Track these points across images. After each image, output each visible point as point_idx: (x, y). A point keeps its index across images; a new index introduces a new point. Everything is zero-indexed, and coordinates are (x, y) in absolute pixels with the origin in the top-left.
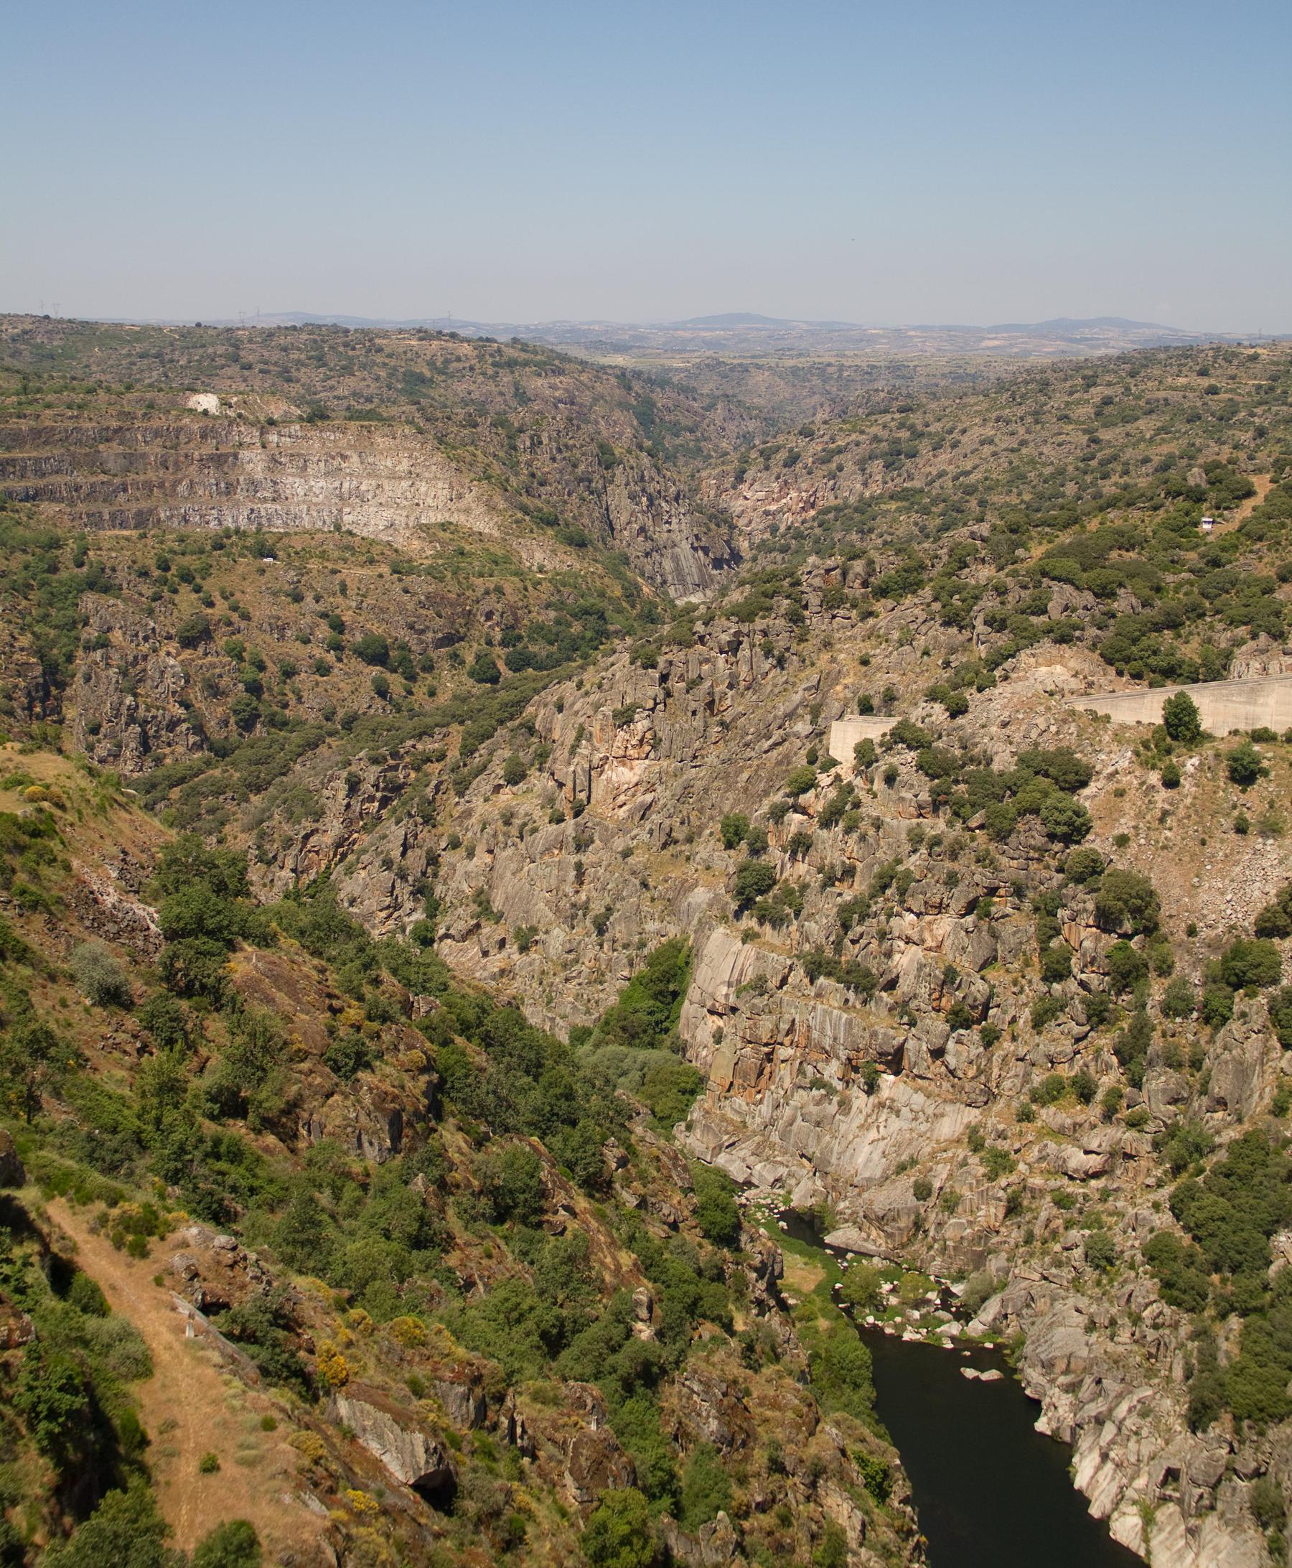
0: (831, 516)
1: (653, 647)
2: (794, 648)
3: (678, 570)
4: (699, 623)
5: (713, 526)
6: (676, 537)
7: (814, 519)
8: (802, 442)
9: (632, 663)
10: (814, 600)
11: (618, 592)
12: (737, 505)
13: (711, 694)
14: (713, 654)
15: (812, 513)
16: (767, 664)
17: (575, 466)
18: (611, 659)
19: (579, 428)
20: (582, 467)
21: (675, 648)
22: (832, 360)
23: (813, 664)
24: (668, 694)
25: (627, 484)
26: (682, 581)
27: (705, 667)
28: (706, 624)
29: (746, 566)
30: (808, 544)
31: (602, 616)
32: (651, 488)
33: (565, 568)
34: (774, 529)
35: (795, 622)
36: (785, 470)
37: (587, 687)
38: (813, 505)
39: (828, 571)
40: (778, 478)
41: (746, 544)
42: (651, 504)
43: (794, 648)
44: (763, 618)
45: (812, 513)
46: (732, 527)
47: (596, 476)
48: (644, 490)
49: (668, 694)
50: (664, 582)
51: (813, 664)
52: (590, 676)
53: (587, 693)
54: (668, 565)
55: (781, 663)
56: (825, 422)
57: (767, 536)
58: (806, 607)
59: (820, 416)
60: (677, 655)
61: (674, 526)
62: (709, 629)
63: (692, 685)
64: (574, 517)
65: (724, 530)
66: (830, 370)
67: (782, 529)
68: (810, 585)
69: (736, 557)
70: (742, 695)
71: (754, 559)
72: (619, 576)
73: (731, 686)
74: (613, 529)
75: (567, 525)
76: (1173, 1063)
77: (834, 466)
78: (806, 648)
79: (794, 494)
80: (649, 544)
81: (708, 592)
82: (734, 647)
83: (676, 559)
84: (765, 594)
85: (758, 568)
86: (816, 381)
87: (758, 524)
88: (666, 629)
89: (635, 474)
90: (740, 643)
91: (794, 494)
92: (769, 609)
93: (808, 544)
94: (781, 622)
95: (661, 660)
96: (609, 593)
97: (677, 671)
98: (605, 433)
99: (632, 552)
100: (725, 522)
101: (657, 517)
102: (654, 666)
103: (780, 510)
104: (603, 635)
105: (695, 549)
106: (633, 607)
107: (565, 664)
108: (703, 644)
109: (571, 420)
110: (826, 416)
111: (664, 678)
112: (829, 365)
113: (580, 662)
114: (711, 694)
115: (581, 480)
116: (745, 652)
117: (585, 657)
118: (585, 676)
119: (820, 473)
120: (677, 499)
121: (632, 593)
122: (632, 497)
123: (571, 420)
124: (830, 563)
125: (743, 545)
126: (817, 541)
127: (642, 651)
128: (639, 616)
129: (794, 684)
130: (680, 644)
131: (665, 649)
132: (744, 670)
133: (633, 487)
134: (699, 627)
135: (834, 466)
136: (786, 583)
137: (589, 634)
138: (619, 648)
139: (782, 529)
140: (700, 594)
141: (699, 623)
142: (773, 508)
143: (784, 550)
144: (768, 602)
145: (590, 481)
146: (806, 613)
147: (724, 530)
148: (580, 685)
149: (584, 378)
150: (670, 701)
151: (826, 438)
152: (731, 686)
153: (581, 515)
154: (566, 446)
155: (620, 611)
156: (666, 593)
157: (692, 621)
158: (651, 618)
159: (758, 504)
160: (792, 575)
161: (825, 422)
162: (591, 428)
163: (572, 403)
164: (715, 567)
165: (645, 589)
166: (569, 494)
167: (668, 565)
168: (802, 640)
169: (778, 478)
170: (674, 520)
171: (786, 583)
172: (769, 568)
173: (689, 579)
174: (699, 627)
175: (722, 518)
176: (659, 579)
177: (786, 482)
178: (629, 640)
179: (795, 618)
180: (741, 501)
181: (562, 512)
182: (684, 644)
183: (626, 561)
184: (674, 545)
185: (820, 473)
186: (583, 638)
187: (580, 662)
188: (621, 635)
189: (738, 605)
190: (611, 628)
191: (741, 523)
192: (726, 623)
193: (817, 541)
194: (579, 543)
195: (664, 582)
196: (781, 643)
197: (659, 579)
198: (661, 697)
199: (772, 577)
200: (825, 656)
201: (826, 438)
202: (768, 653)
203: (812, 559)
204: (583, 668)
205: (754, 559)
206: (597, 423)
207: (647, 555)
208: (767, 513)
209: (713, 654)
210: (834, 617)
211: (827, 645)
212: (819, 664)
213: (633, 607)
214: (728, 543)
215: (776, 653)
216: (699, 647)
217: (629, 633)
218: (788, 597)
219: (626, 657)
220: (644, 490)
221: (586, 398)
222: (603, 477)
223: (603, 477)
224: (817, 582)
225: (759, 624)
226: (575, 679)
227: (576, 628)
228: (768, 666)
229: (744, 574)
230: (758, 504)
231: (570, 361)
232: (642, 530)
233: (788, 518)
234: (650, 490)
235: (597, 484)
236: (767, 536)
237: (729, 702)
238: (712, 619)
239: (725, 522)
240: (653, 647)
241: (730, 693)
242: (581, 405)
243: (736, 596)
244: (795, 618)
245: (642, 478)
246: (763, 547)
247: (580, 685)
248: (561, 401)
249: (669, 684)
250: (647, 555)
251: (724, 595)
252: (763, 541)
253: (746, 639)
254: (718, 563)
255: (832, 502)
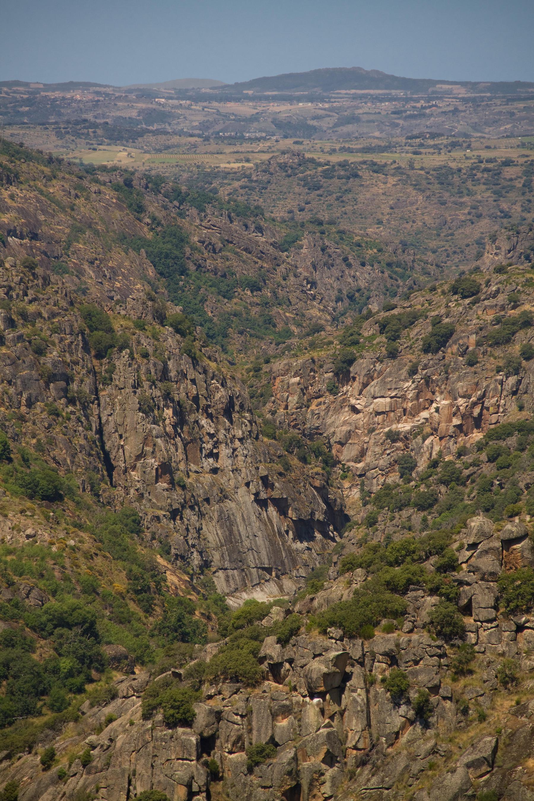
0: (512, 441)
1: (186, 685)
2: (448, 685)
3: (231, 540)
4: (270, 640)
5: (295, 461)
6: (227, 480)
7: (480, 446)
8: (458, 306)
9: (146, 717)
10: (482, 596)
11: (121, 584)
12: (339, 423)
13: (294, 773)
14: (297, 698)
15: (477, 436)
16: (397, 718)
17: (40, 352)
18: (108, 710)
19: (46, 281)
20: (54, 354)
21: (227, 688)
22: (514, 154)
23: (482, 718)
24: (215, 775)
25: (137, 385)
26: (237, 559)
27: (283, 723)
28: (283, 642)
29: (356, 534)
30: (469, 493)
31: (90, 630)
32: (182, 392)
33: (23, 540)
34: (406, 467)
35: (448, 638)
36: (426, 358)
37: (62, 763)
38: (478, 422)
39: (508, 543)
40: (413, 372)
41: (355, 494)
42: (181, 419)
43: (448, 685)
44: (389, 630)
45: (477, 436)
46: (330, 462)
47: (79, 371)
48: (167, 396)
49: (215, 775)
50: (206, 565)
51: (482, 718)
52: (68, 743)
53: (62, 777)
54: (213, 533)
55: (422, 714)
56: (500, 270)
57: (394, 478)
58: (467, 610)
59: (490, 259)
60: (230, 701)
61: (224, 462)
62: (290, 652)
63: (260, 756)
64: (39, 447)
65: (315, 467)
66: (509, 172)
67: (422, 465)
68: (474, 570)
69: (337, 518)
70: (352, 776)
71: (371, 522)
72: (123, 554)
73: (330, 759)
74: (110, 468)
75: (25, 460)
76: (499, 767)
77: (516, 349)
78: (471, 686)
79: (442, 402)
80: (178, 495)
81: (288, 584)
82: (335, 685)
83: (227, 521)
84: (392, 587)
85: (378, 538)
86: (483, 194)
87: (377, 457)
88: (210, 652)
89: (152, 365)
90: (347, 677)
91: (442, 402)
92: (400, 614)
93: (469, 493)
94: (422, 638)
95: (201, 711)
96: (103, 587)
97: (229, 731)
98: (94, 291)
99: (147, 510)
100: (318, 453)
101: (192, 445)
102: (187, 722)
103: (417, 432)
104: (92, 664)
105: (262, 503)
106: (149, 611)
107: (20, 721)
108: (279, 679)
109: (31, 267)
110: (501, 259)
111: (206, 744)
112: (508, 163)
113: (49, 716)
114: (294, 773)
115: (51, 378)
116: (355, 694)
117: (58, 706)
118: (59, 743)
119: (491, 363)
120: (228, 412)
121: (146, 587)
122: (147, 408)
123: (31, 267)
124: (512, 528)
125: (352, 495)
126: (487, 488)
127: (165, 695)
128: (160, 629)
129: (448, 756)
130: (235, 679)
131: (208, 689)
132: (354, 727)
133: (147, 390)
134: (271, 648)
135: (516, 349)
136: (430, 565)
137: (66, 664)
138: (123, 688)
139: (422, 465)
140: (272, 587)
141: (270, 640)
142: (405, 426)
143: (426, 504)
144: (397, 601)
145: (68, 380)
146: (469, 621)
147: (315, 467)
148: (49, 760)
149: (55, 189)
150: (217, 787)
151: (501, 299)
152: (330, 759)
153: (52, 441)
154: (24, 315)
155: (123, 620)
156: (210, 585)
157: (257, 637)
158: (182, 633)
159: (377, 420)
160: (440, 550)
161: (500, 270)
162: (69, 282)
163: (34, 237)
164: (300, 536)
165: (171, 578)
166: (30, 404)
167: (213, 533)
168: (462, 671)
169: (413, 372)
170: (224, 451)
171: (430, 565)
172: (398, 538)
173: (251, 559)
174: (271, 648)
175: (310, 446)
176: (196, 560)
177: (428, 380)
178: (141, 674)
179: (449, 631)
180: (346, 415)
181: (16, 438)
182: (242, 679)
183: (136, 526)
184: (224, 496)
185: (491, 363)
186: (56, 671)
187: (49, 716)
188: (126, 663)
189: (342, 606)
190: (108, 651)
191: (347, 454)
192: (321, 641)
193: (487, 488)
194: (50, 495)
195: (206, 565)
196: (423, 676)
197: (196, 560)
198: (200, 780)
199: (404, 555)
200: (506, 703)
201: (501, 299)
202: (399, 696)
203: (477, 522)
204: (54, 727)
205: (371, 522)
206: (80, 273)
207: (175, 514)
208: (393, 437)
209: (297, 698)
210: (520, 628)
211: (509, 680)
212: (494, 716)
213: (149, 611)
214: (322, 491)
215: (414, 695)
216: (270, 684)
217: (140, 661)
218: (434, 591)
219: (136, 705)
220: (167, 396)
221: (59, 226)
222: (92, 372)
223: (92, 372)
224: (488, 563)
225: (382, 641)
226: (40, 749)
227: (43, 652)
228: (398, 721)
229: (352, 550)
230: (377, 420)
231: (28, 157)
232: (165, 469)
233: (432, 445)
234: (180, 395)
235: (81, 385)
236: (394, 478)
237: (326, 789)
238: (294, 632)
239: (318, 453)
240: (186, 685)
241: (330, 772)
242: (51, 240)
243: (339, 590)
244: (449, 631)
245: (164, 374)
246: (387, 499)
247: (49, 760)
248: (12, 232)
249: (216, 755)
250: (175, 514)
251: (316, 589)
252: (386, 487)
253: (357, 670)
254: (304, 529)
255: (514, 415)
